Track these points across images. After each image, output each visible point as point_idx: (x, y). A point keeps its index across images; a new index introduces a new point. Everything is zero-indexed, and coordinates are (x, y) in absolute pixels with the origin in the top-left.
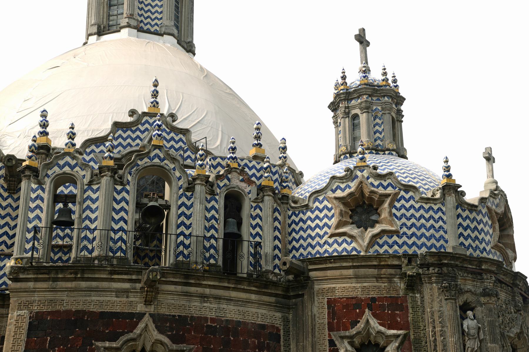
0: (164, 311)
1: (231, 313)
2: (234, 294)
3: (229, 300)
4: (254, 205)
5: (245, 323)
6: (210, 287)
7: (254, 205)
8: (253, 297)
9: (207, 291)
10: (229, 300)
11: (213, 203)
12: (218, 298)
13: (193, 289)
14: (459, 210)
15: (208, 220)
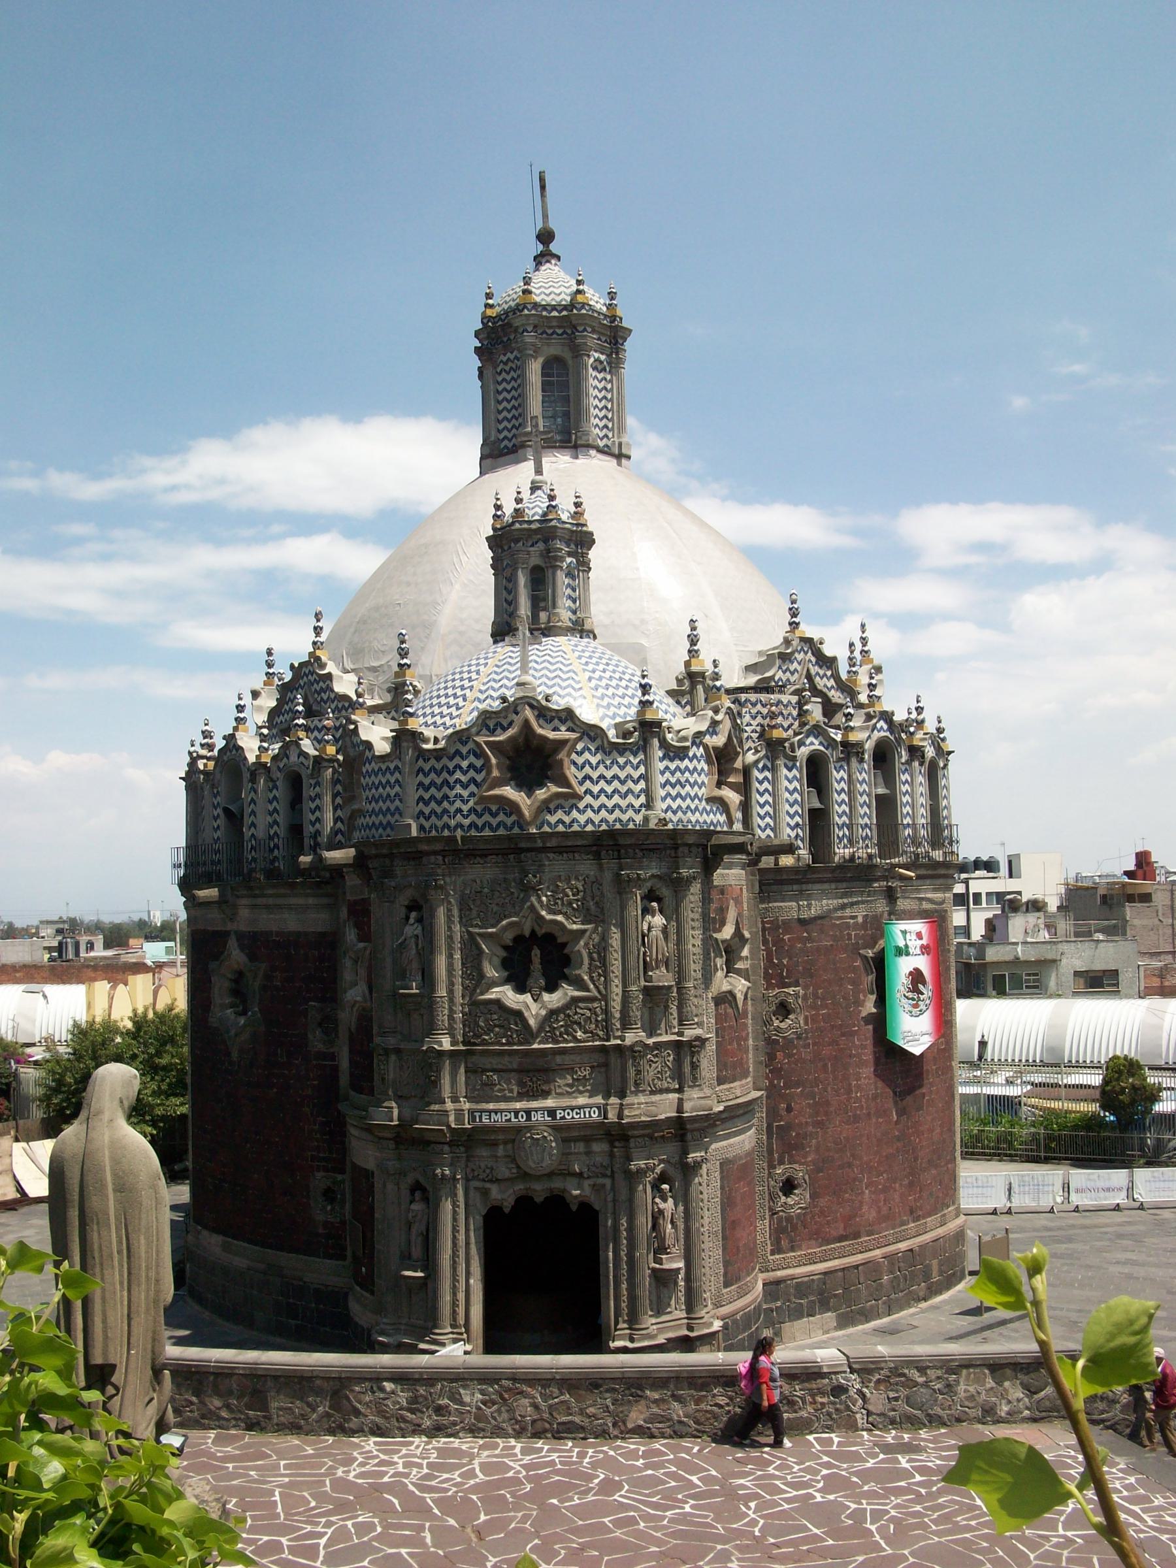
0: (243, 928)
1: (291, 923)
2: (293, 901)
3: (289, 907)
4: (313, 782)
5: (306, 934)
6: (271, 896)
7: (313, 782)
8: (311, 901)
9: (271, 901)
10: (289, 907)
11: (275, 791)
12: (279, 907)
13: (259, 901)
14: (421, 762)
15: (271, 814)
